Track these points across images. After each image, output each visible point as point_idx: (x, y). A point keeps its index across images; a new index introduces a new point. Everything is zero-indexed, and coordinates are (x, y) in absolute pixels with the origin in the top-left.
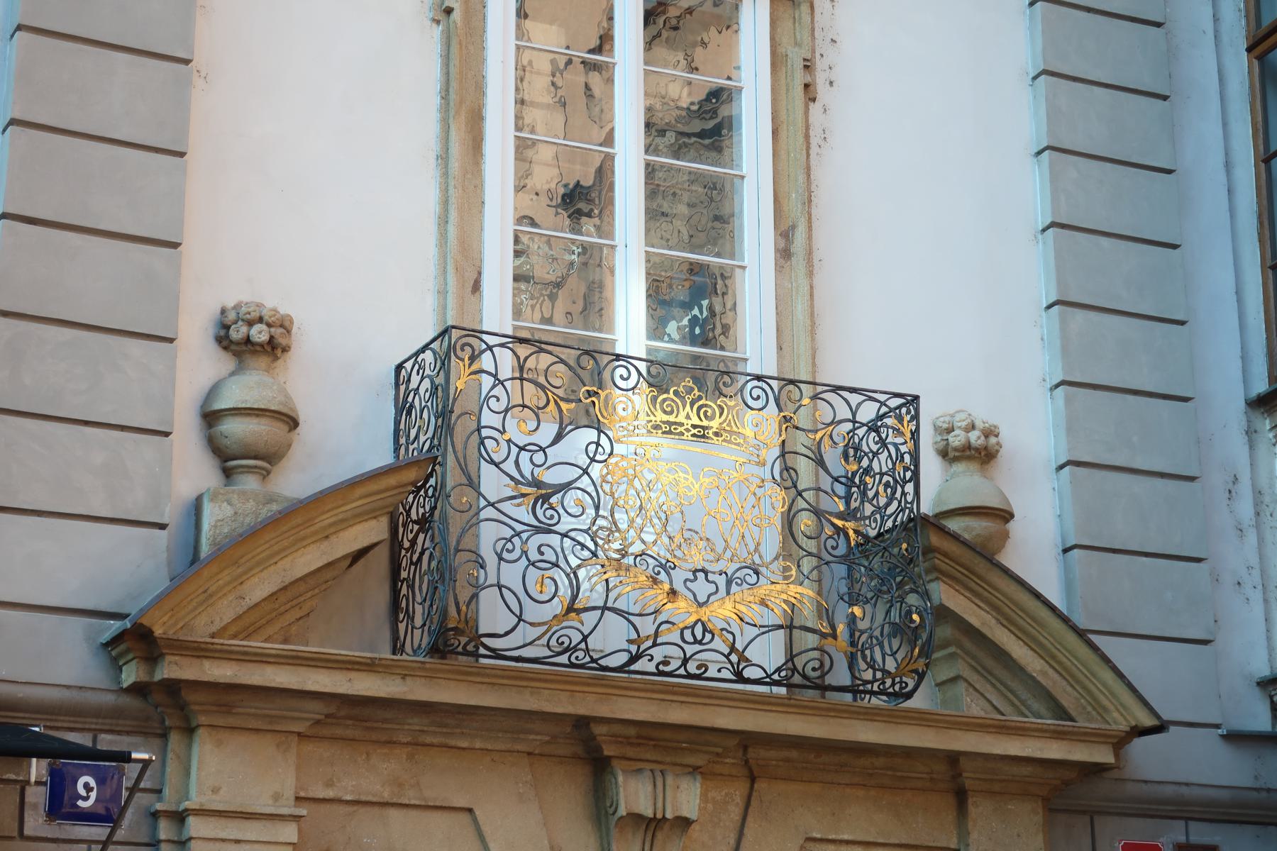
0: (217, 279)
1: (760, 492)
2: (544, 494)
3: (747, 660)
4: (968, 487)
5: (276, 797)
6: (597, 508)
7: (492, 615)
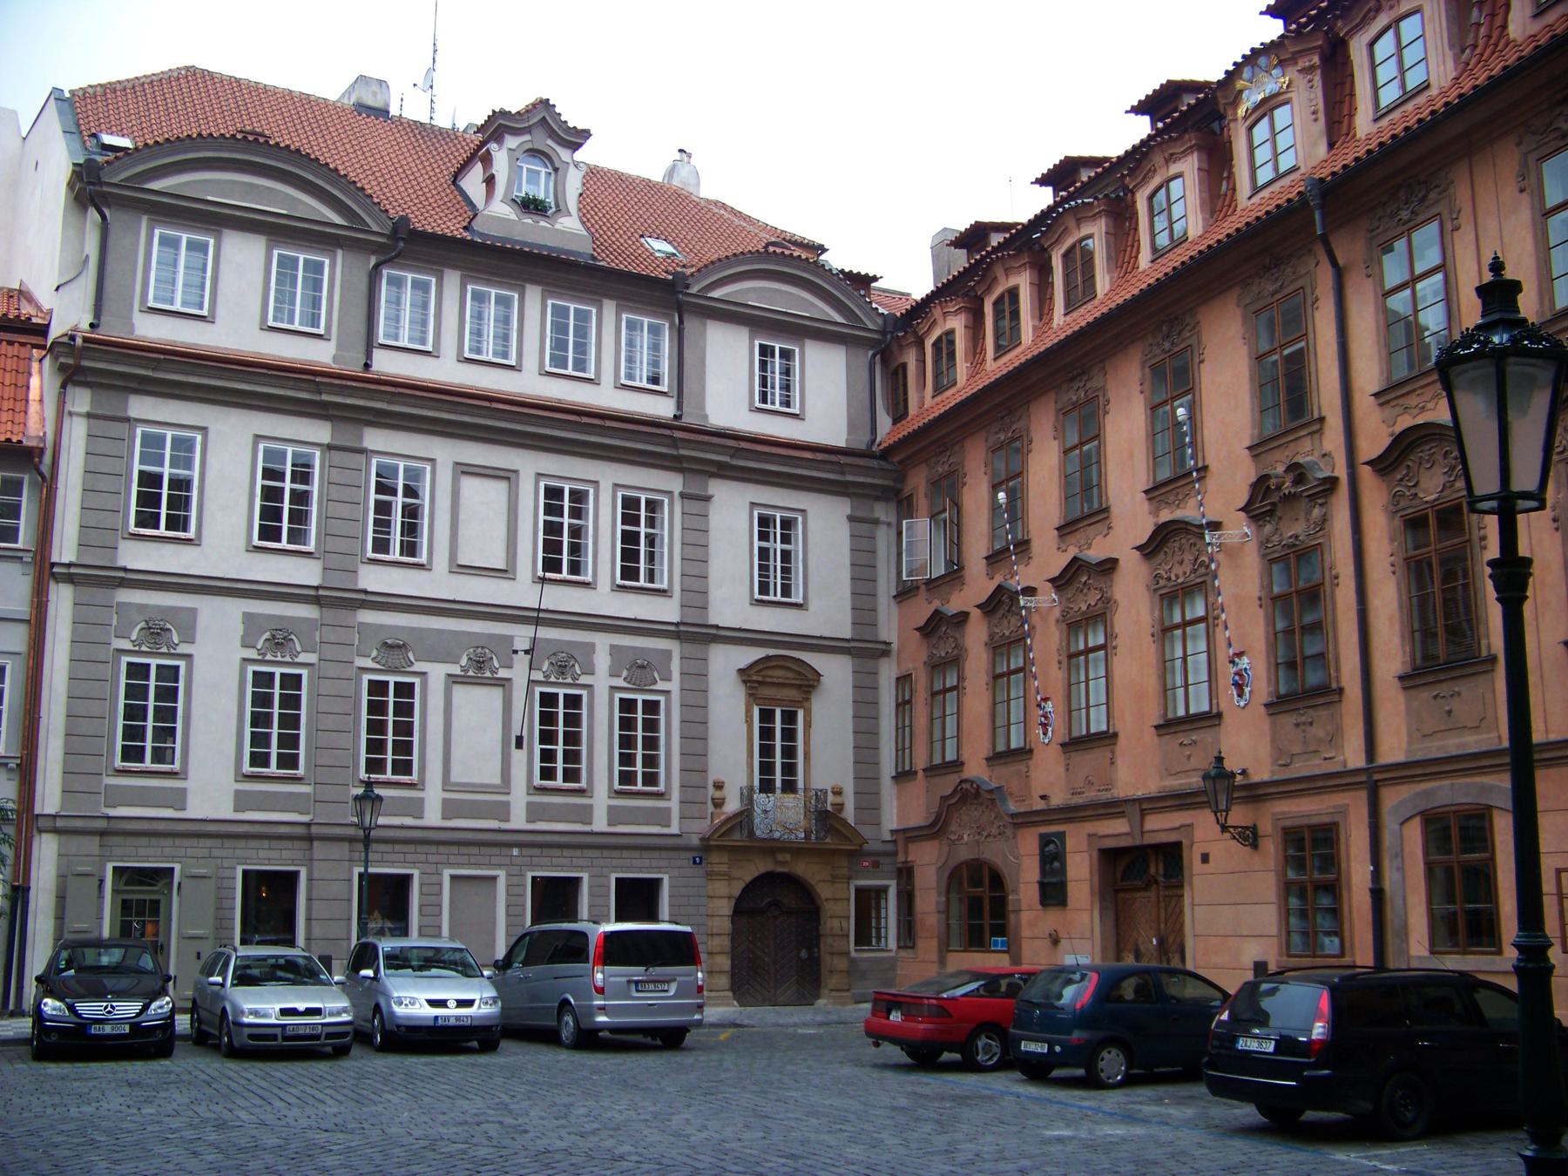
0: (713, 776)
2: (766, 812)
4: (838, 800)
7: (758, 833)
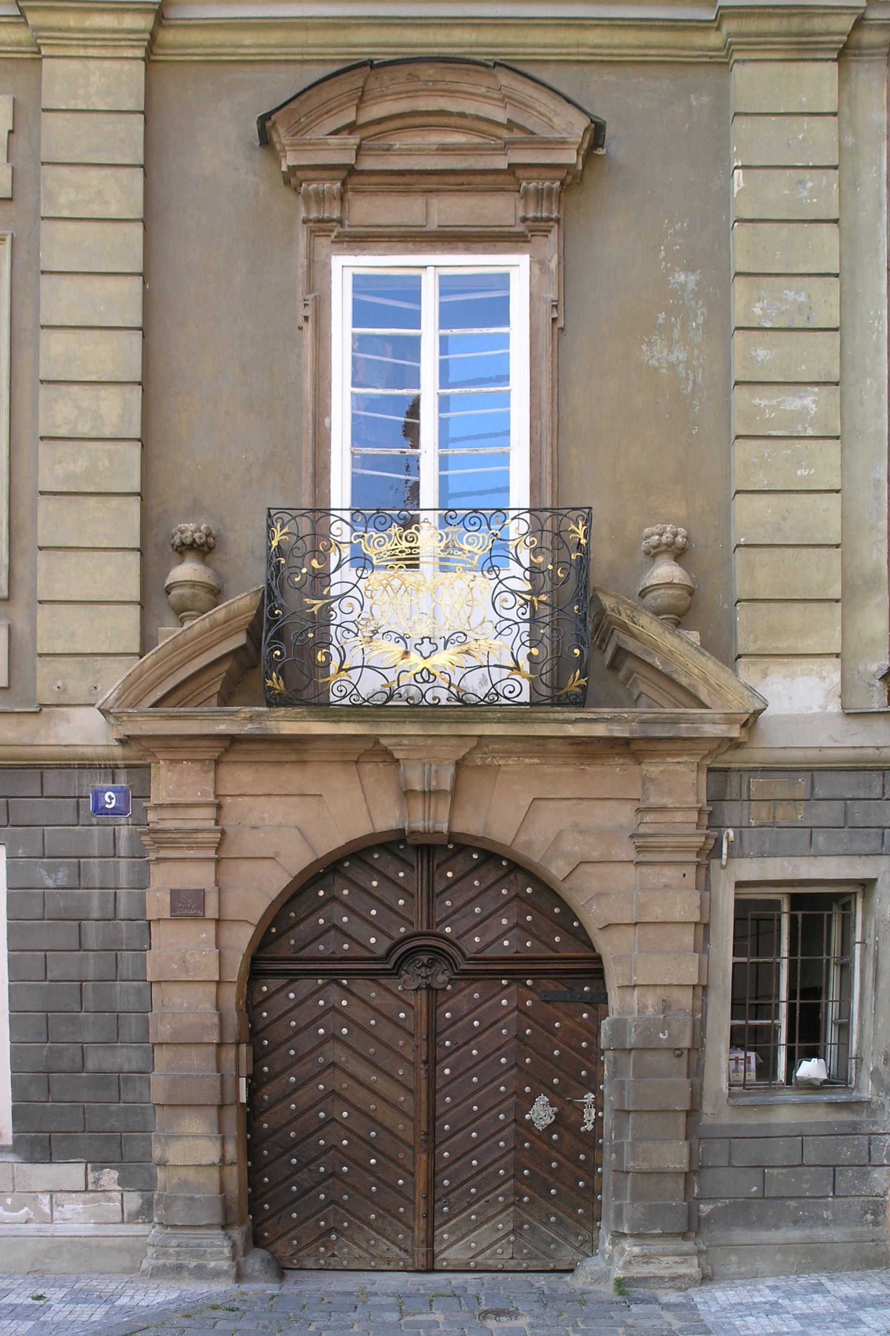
1: (472, 584)
3: (463, 691)
5: (203, 792)
6: (362, 607)
